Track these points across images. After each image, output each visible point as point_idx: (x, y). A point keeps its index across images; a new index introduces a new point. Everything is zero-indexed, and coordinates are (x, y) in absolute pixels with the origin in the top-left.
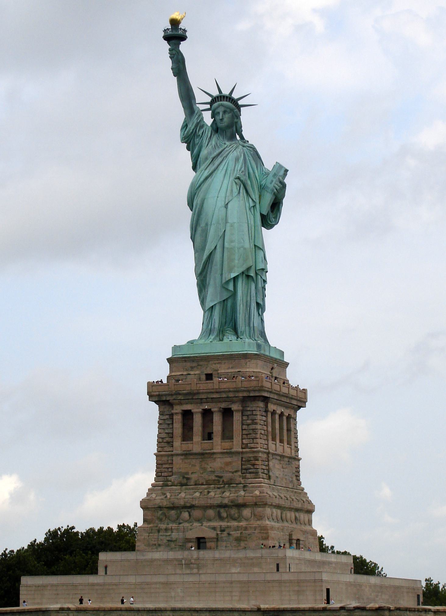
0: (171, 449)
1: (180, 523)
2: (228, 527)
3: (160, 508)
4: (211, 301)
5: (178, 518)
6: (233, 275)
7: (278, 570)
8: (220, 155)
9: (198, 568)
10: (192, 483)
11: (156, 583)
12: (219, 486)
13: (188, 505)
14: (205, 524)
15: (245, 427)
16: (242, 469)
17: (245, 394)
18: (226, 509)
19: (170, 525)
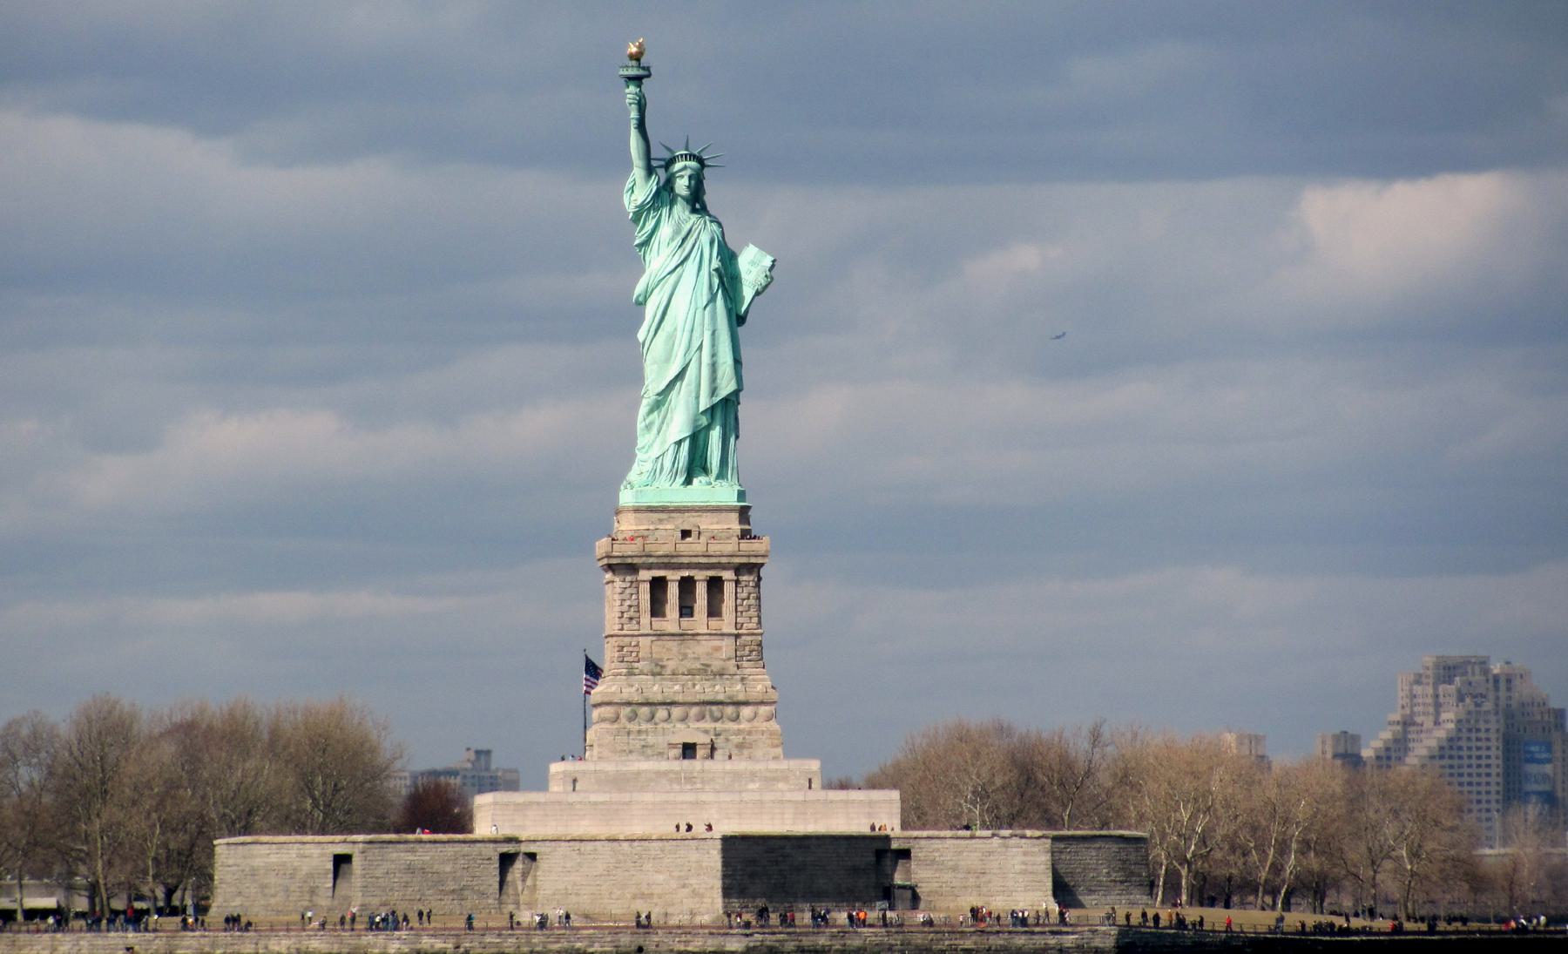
0: (636, 627)
1: (656, 724)
2: (725, 731)
3: (629, 704)
4: (680, 432)
5: (653, 717)
6: (716, 399)
7: (810, 787)
8: (691, 235)
9: (703, 782)
10: (669, 672)
11: (682, 803)
12: (707, 677)
13: (668, 701)
14: (692, 725)
15: (739, 601)
16: (736, 656)
17: (744, 560)
18: (721, 707)
19: (644, 726)
